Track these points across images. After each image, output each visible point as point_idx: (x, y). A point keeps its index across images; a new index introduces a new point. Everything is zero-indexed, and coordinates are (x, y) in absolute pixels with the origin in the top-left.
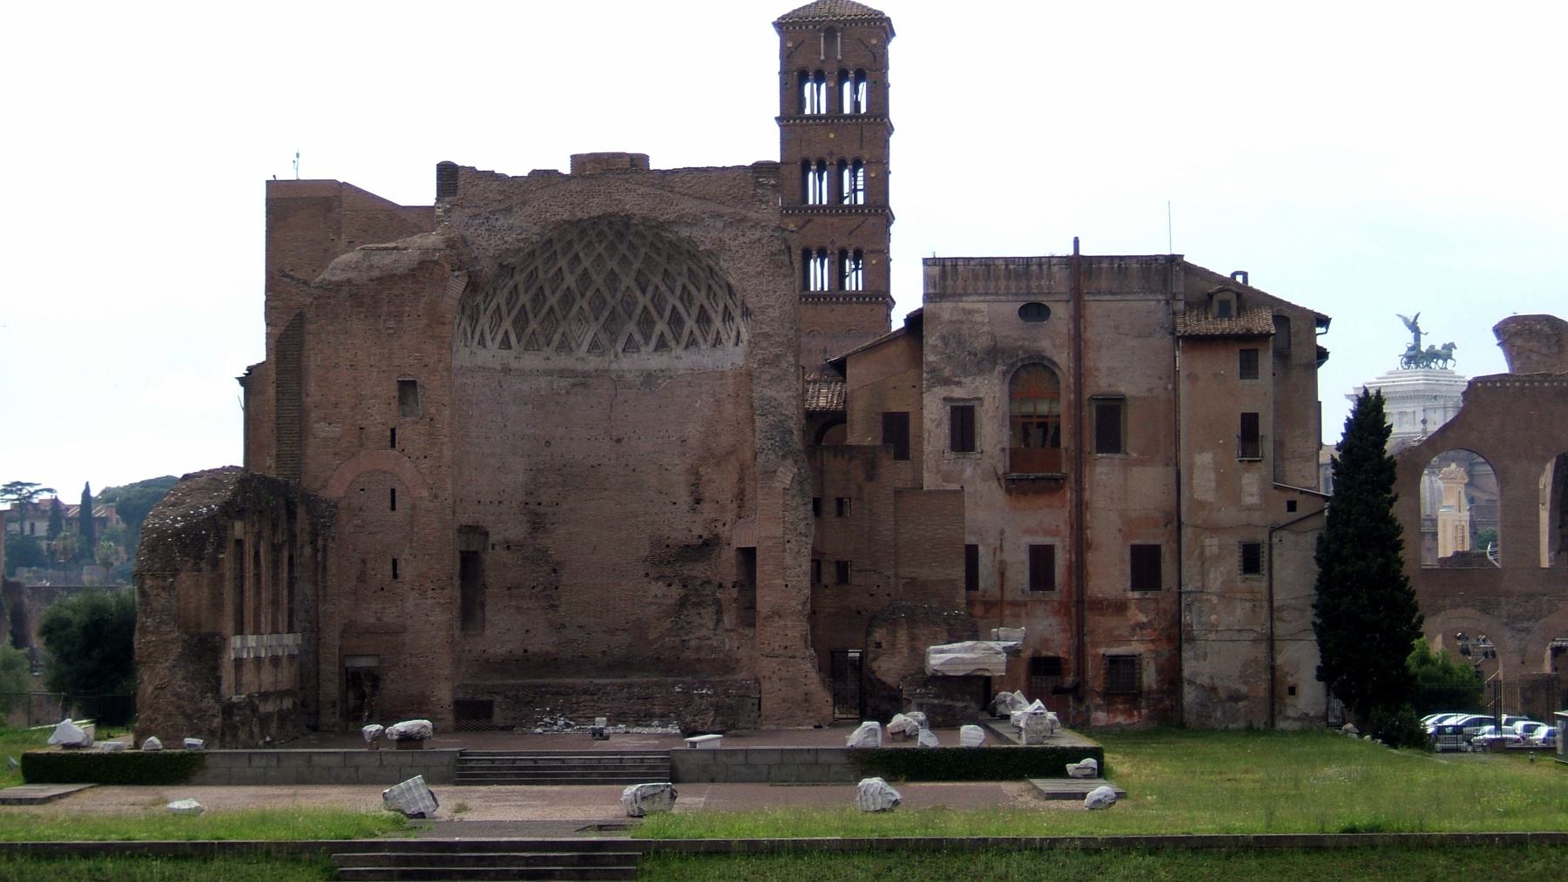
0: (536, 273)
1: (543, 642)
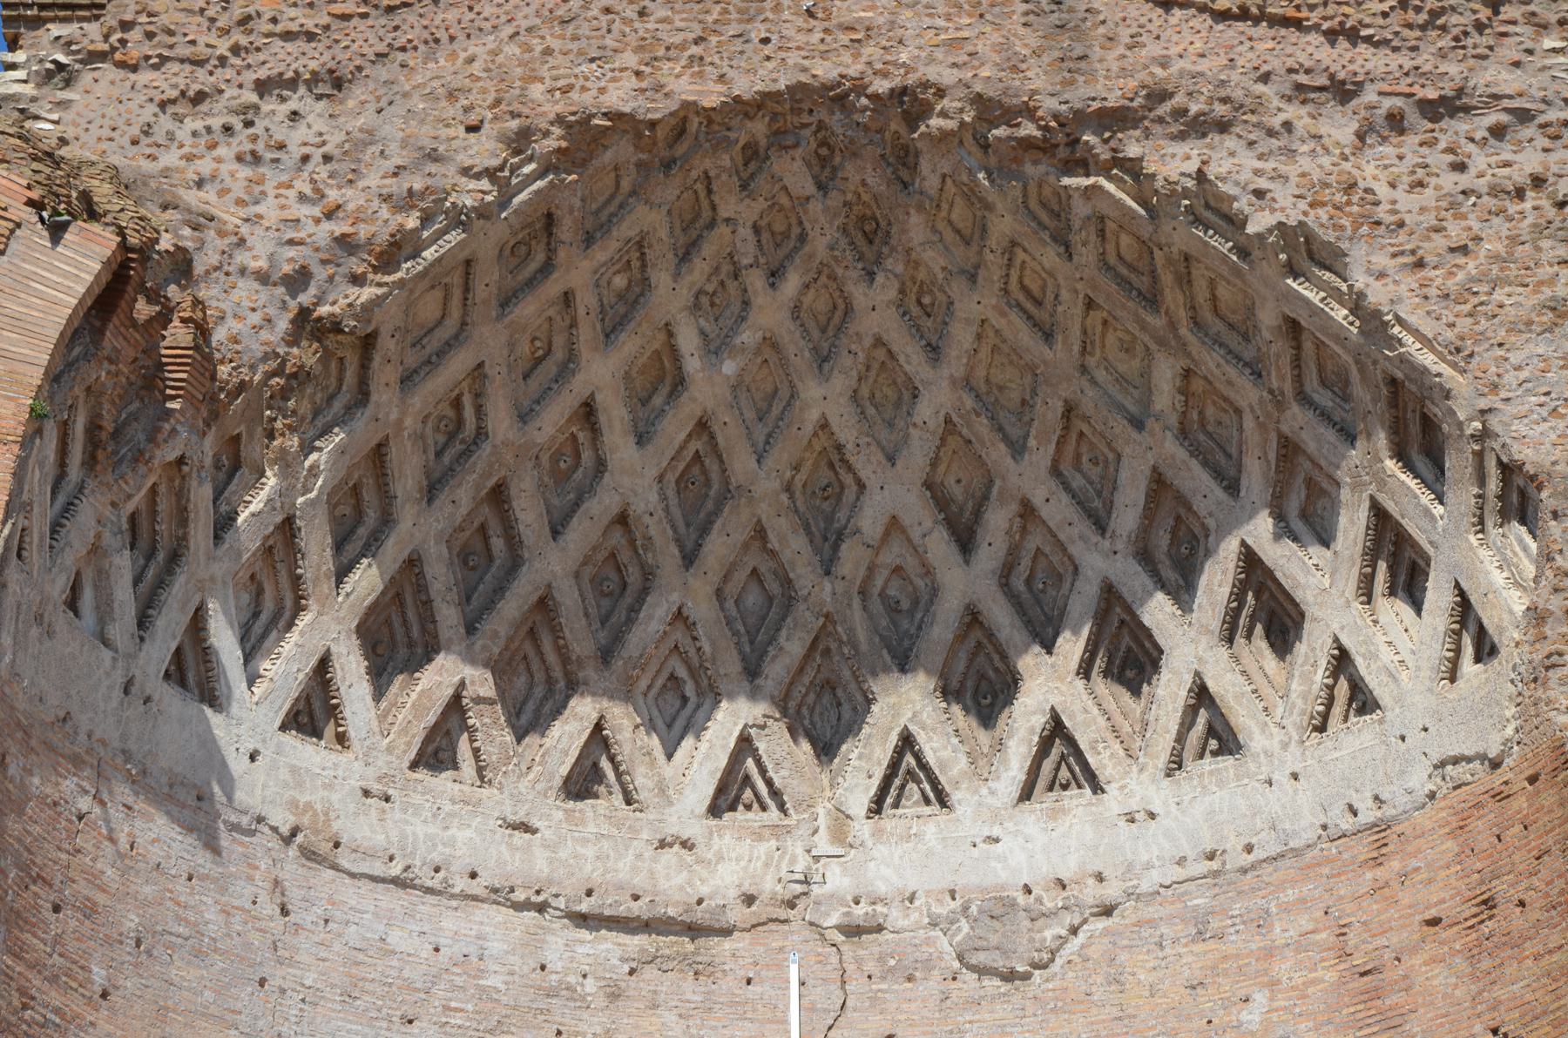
0: (479, 410)
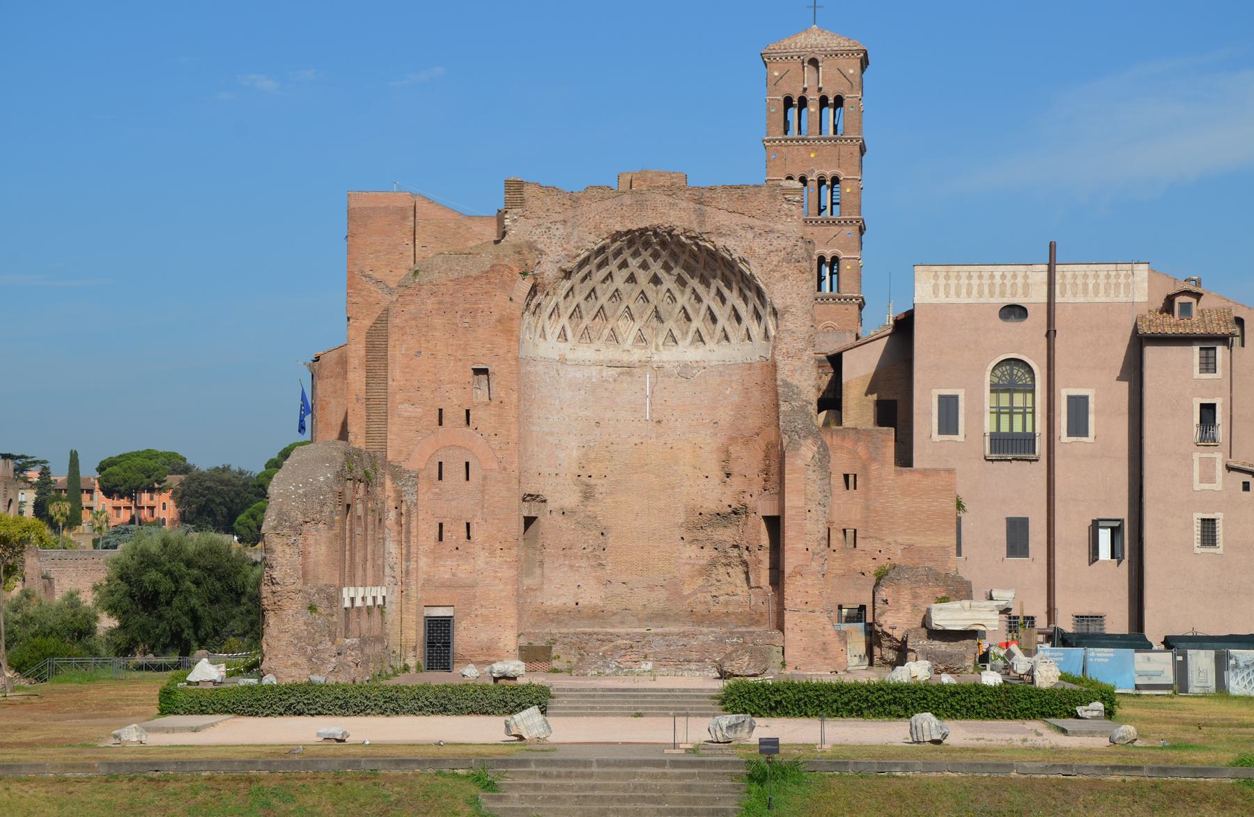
1: (592, 596)
